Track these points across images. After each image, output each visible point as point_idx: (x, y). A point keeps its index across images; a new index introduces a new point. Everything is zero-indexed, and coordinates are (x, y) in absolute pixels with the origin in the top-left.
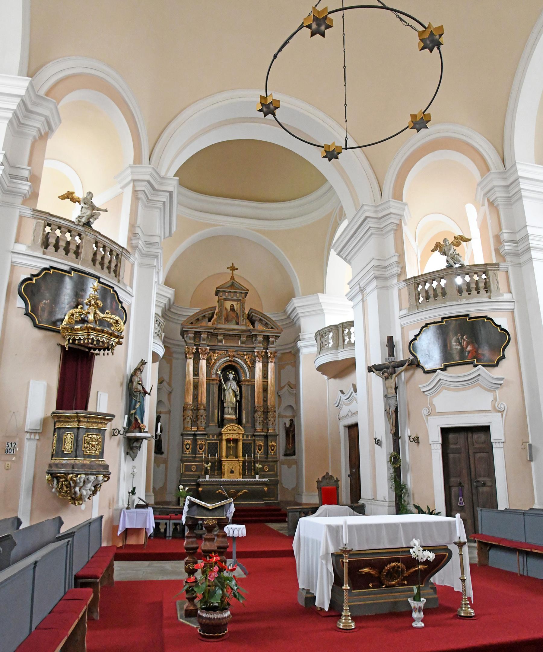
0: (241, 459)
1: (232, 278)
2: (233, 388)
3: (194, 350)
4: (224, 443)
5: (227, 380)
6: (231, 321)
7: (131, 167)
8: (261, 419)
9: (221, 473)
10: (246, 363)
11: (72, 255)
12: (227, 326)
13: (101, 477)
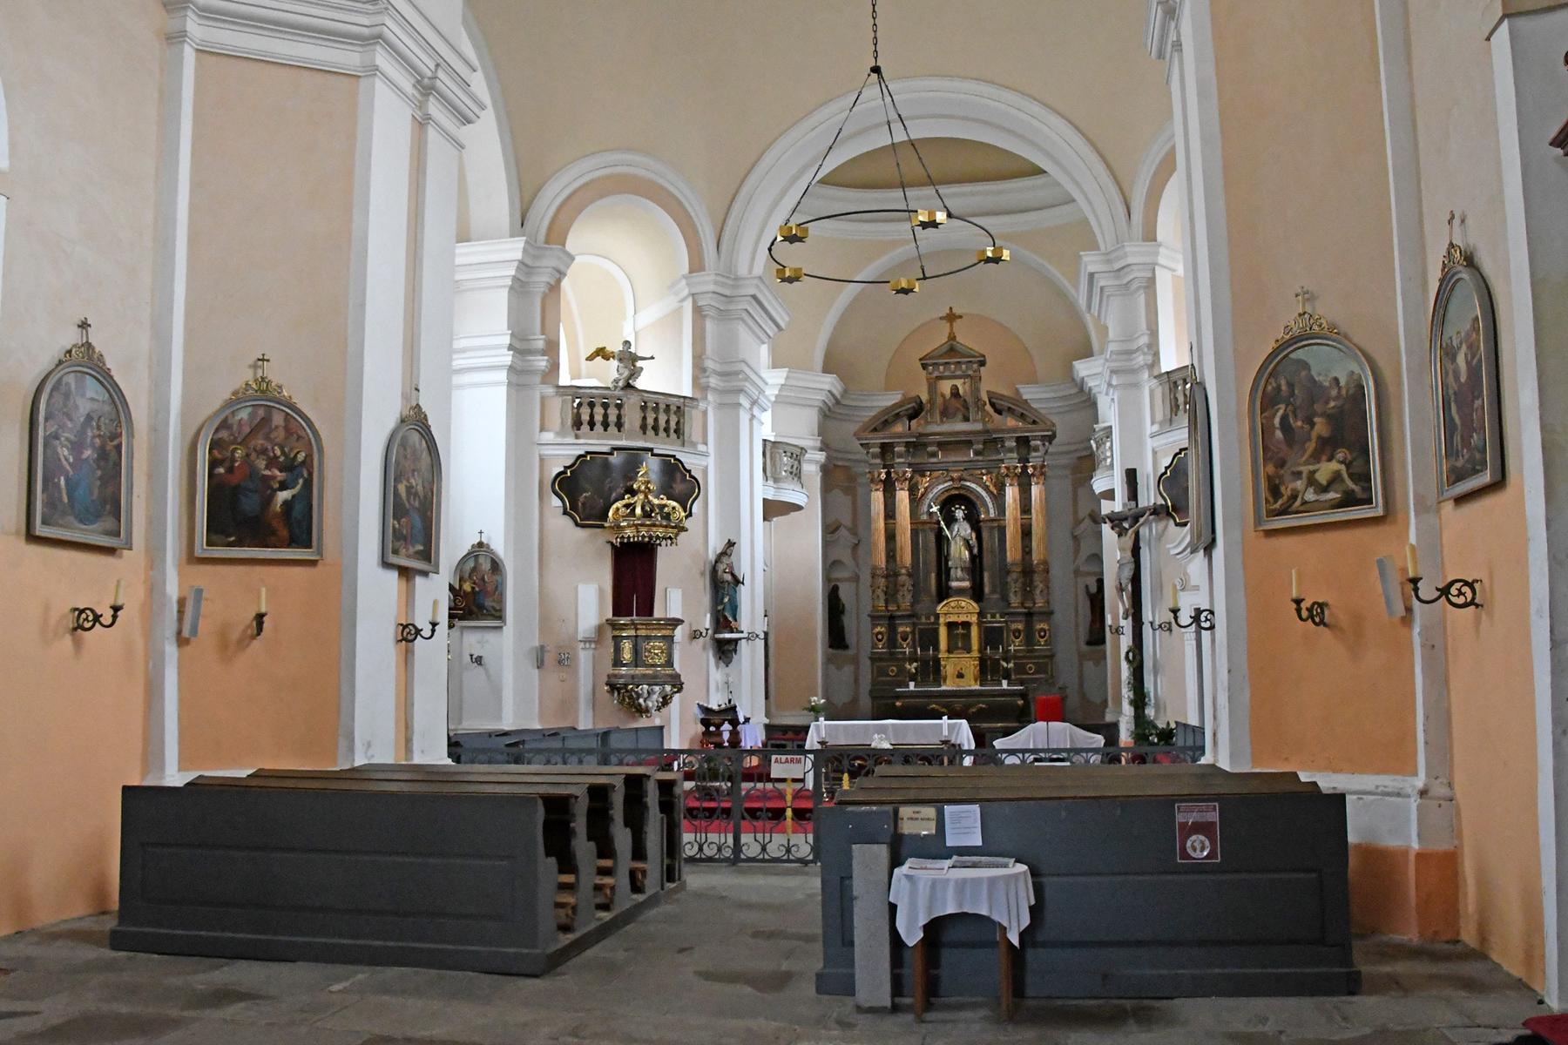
0: (975, 654)
1: (952, 337)
2: (963, 533)
3: (883, 476)
4: (943, 632)
5: (950, 520)
6: (954, 415)
7: (684, 277)
8: (1019, 584)
9: (938, 677)
10: (986, 489)
11: (612, 429)
12: (947, 427)
13: (668, 688)
